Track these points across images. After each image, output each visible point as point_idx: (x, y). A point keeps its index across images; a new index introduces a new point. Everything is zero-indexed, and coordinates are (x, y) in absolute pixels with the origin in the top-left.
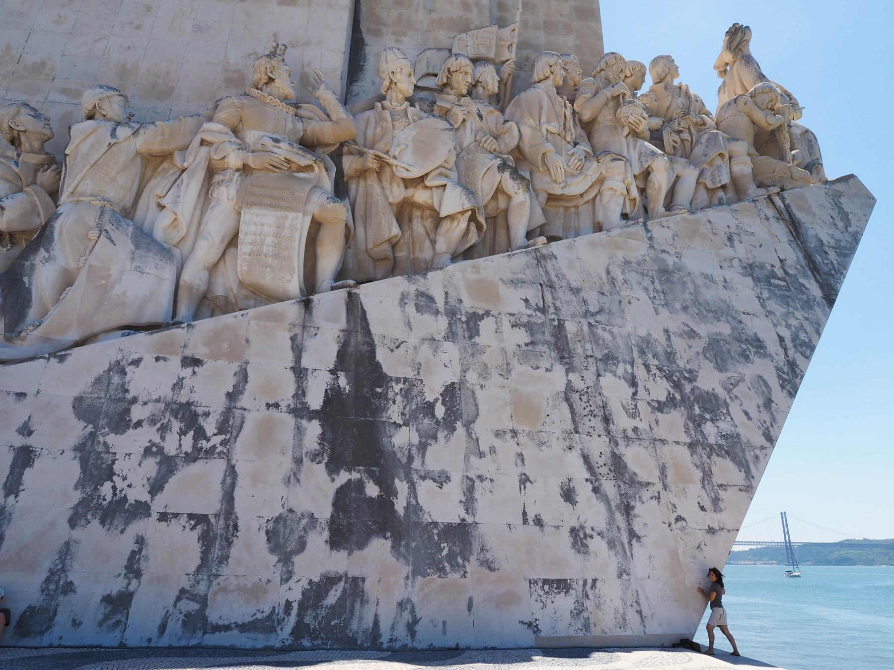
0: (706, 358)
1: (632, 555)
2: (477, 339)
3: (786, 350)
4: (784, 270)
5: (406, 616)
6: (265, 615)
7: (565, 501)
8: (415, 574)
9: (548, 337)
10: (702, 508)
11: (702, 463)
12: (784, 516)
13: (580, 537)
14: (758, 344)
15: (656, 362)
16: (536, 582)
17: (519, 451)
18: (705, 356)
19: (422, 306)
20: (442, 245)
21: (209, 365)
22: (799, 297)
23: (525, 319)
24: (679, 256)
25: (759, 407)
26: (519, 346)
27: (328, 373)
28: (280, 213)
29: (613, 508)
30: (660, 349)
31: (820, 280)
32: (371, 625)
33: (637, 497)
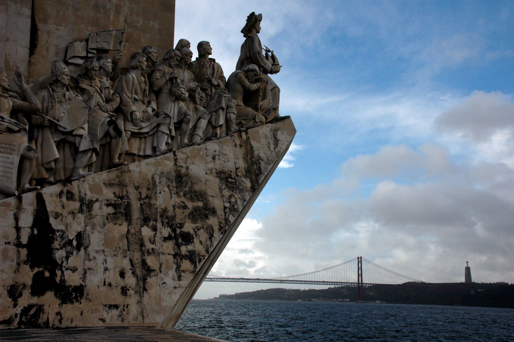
0: (189, 218)
1: (143, 296)
3: (225, 213)
5: (59, 317)
6: (8, 318)
7: (121, 277)
8: (62, 303)
9: (122, 210)
10: (174, 280)
11: (177, 262)
12: (360, 260)
13: (125, 291)
15: (166, 220)
16: (106, 305)
17: (105, 258)
19: (69, 198)
20: (78, 164)
23: (113, 202)
24: (187, 168)
25: (207, 239)
28: (5, 155)
29: (139, 279)
31: (253, 179)
32: (46, 320)
33: (149, 275)
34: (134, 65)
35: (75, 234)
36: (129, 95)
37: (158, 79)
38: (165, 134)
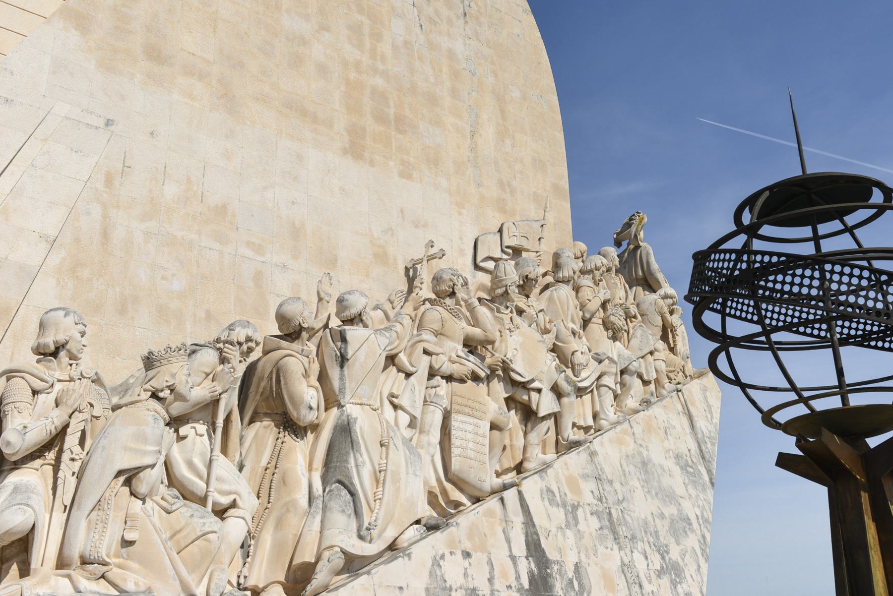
0: (671, 535)
2: (580, 527)
3: (700, 525)
4: (691, 459)
9: (607, 523)
14: (688, 520)
18: (670, 533)
21: (475, 555)
22: (700, 481)
26: (596, 530)
27: (525, 559)
28: (476, 421)
30: (652, 529)
34: (567, 276)
35: (573, 568)
36: (566, 323)
37: (590, 301)
38: (611, 391)
